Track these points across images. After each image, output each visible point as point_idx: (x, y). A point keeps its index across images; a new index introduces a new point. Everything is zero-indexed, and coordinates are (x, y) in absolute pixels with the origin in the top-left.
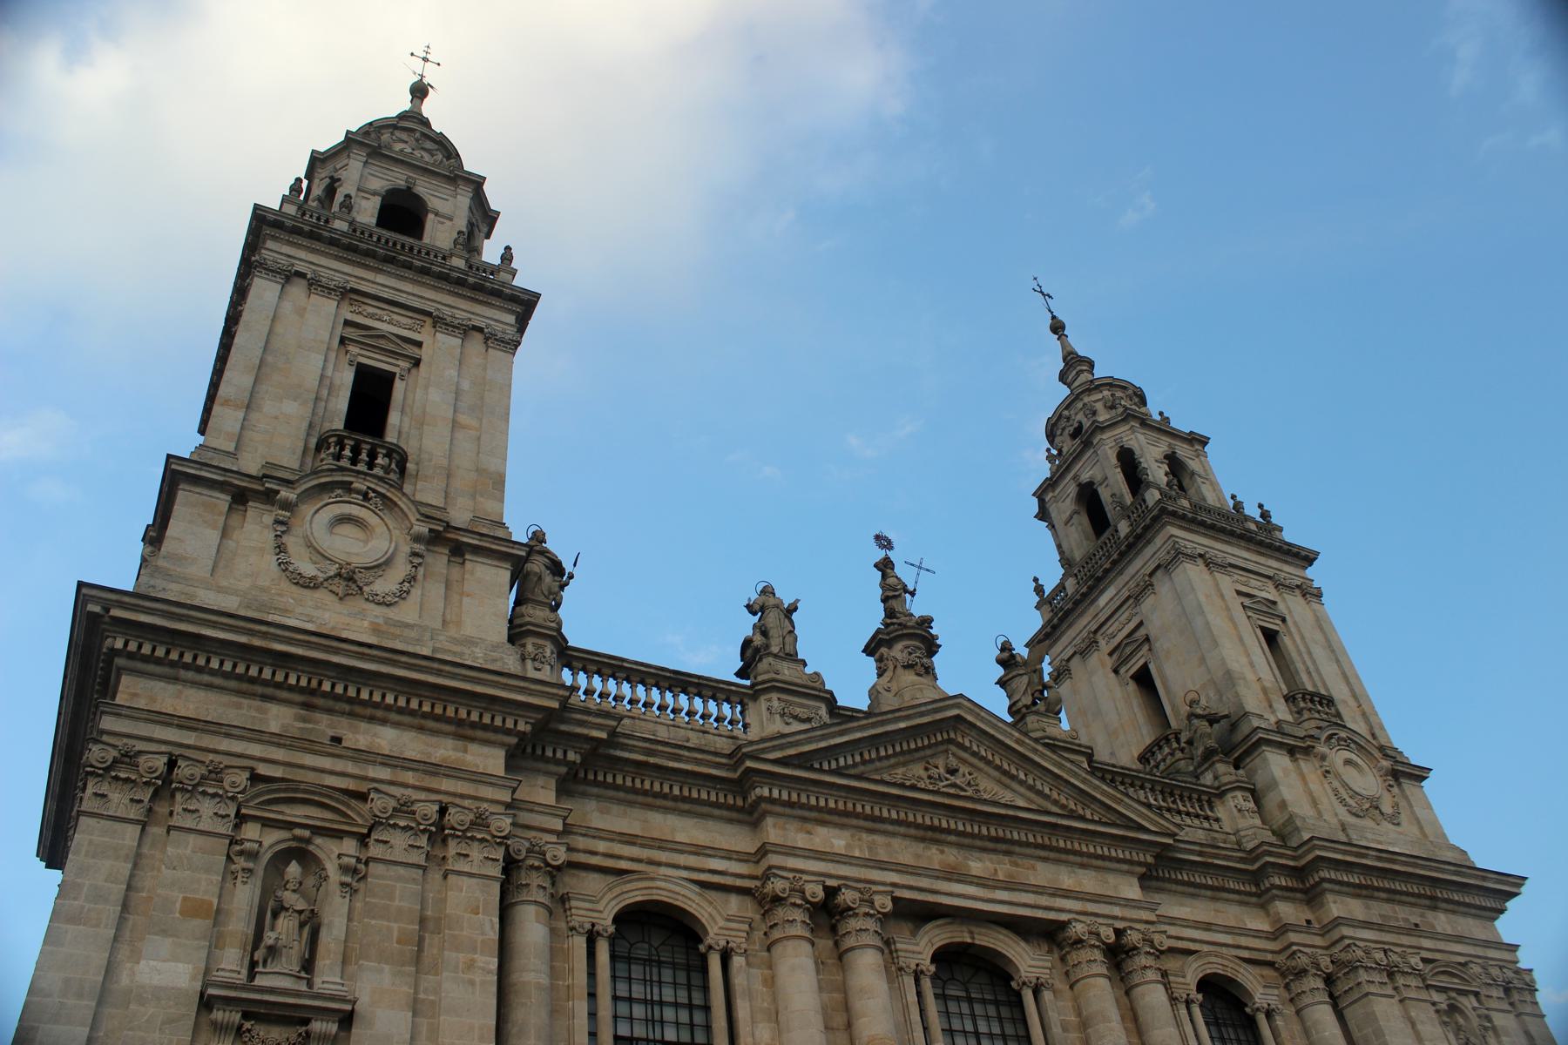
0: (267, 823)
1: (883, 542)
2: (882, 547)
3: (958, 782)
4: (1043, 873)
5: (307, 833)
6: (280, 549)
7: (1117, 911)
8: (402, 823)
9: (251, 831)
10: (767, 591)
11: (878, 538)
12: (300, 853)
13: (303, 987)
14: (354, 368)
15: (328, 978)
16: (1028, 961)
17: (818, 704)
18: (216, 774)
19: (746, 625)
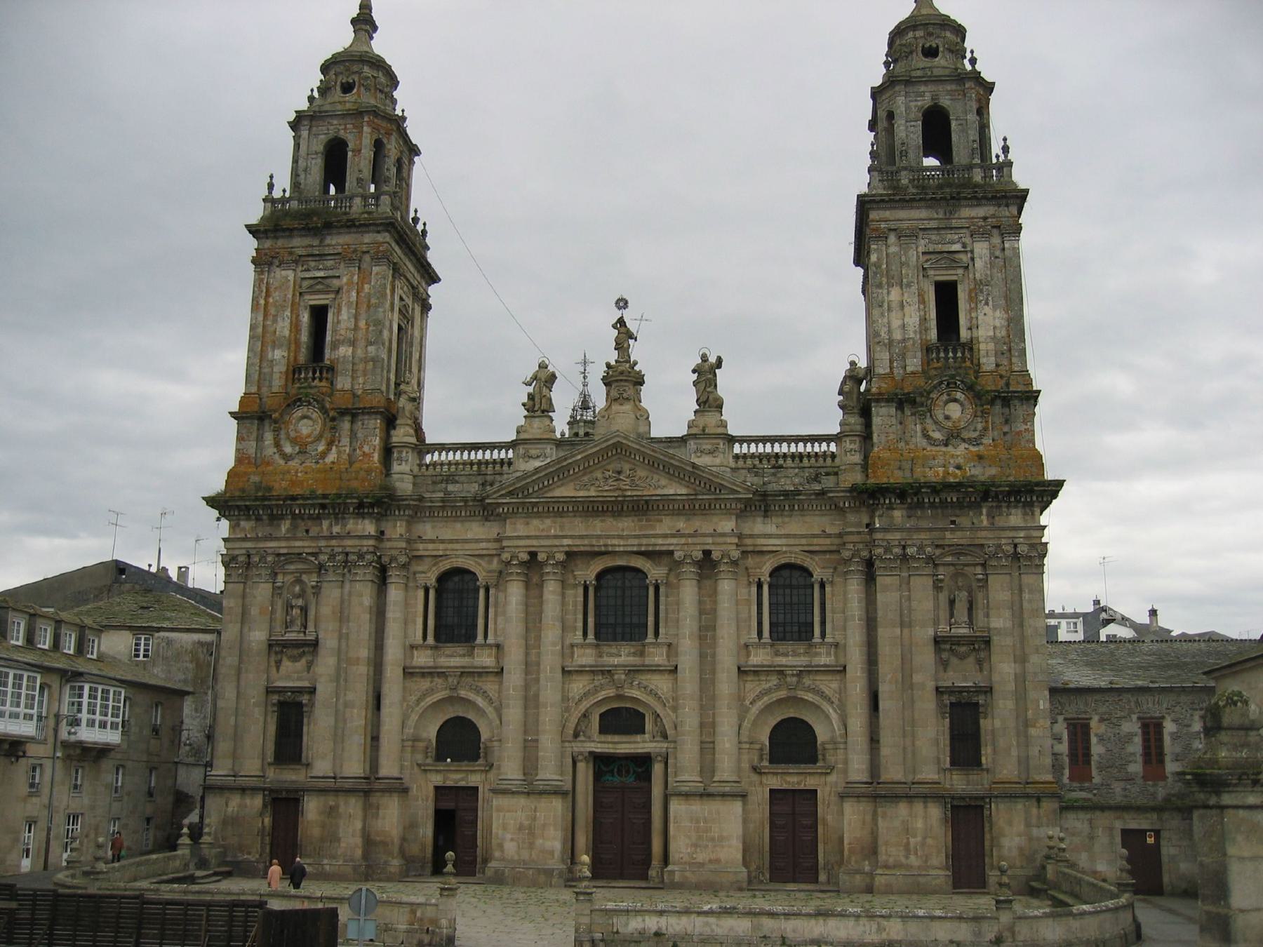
0: (284, 573)
1: (622, 303)
2: (619, 308)
3: (621, 477)
4: (666, 525)
5: (298, 575)
6: (277, 444)
7: (710, 540)
8: (331, 564)
9: (280, 578)
10: (543, 366)
11: (617, 302)
12: (299, 581)
13: (301, 636)
14: (308, 310)
15: (311, 628)
16: (655, 572)
17: (545, 446)
18: (263, 558)
19: (522, 394)
